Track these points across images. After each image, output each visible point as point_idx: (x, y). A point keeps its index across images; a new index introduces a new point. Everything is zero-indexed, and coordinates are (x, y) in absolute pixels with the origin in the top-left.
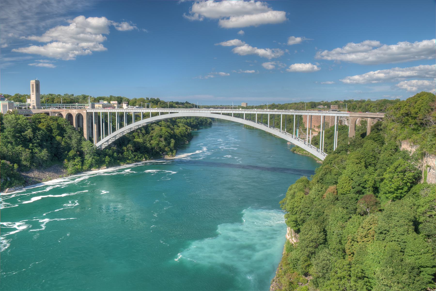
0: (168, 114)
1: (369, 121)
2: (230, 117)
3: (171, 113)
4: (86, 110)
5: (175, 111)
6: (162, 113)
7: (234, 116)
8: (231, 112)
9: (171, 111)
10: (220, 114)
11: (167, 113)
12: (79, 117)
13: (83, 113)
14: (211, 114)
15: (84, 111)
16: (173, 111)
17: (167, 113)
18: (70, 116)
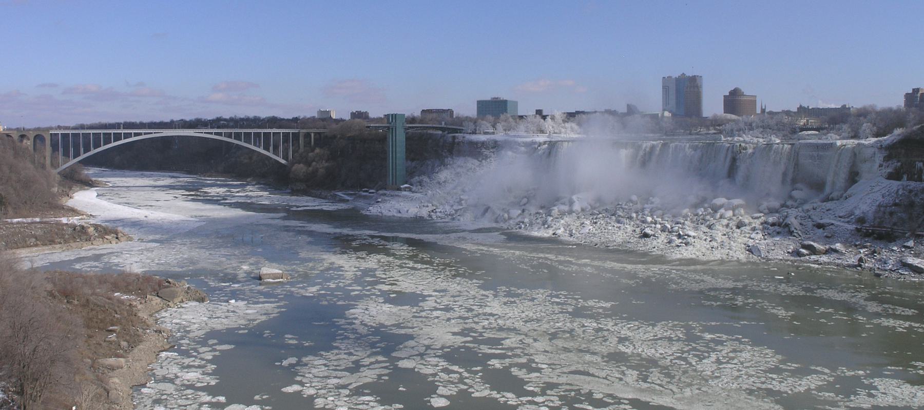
2: (211, 135)
3: (155, 133)
6: (145, 134)
7: (214, 134)
10: (202, 133)
11: (152, 133)
17: (152, 133)
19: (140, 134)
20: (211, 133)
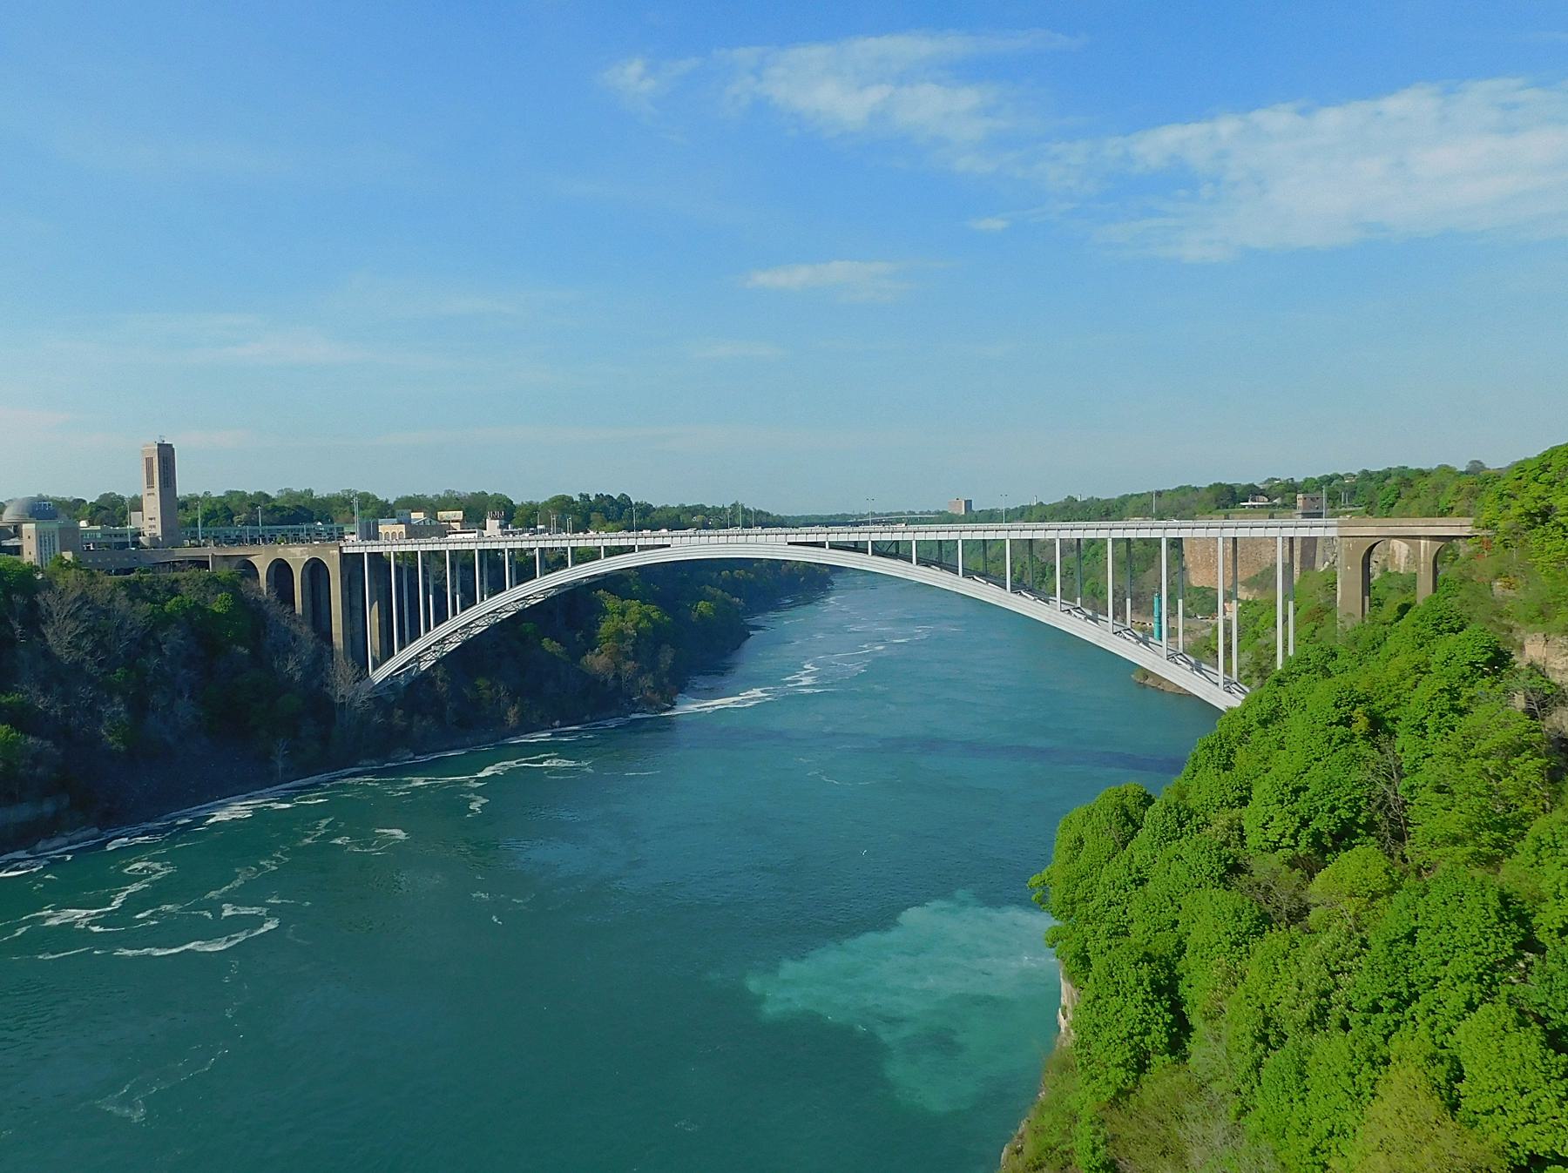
0: (634, 551)
1: (1425, 552)
3: (642, 548)
4: (341, 547)
5: (659, 542)
6: (612, 552)
8: (864, 537)
9: (641, 542)
10: (821, 545)
11: (631, 549)
12: (316, 569)
14: (790, 547)
15: (331, 552)
17: (631, 549)
18: (281, 569)
19: (591, 555)
20: (857, 547)
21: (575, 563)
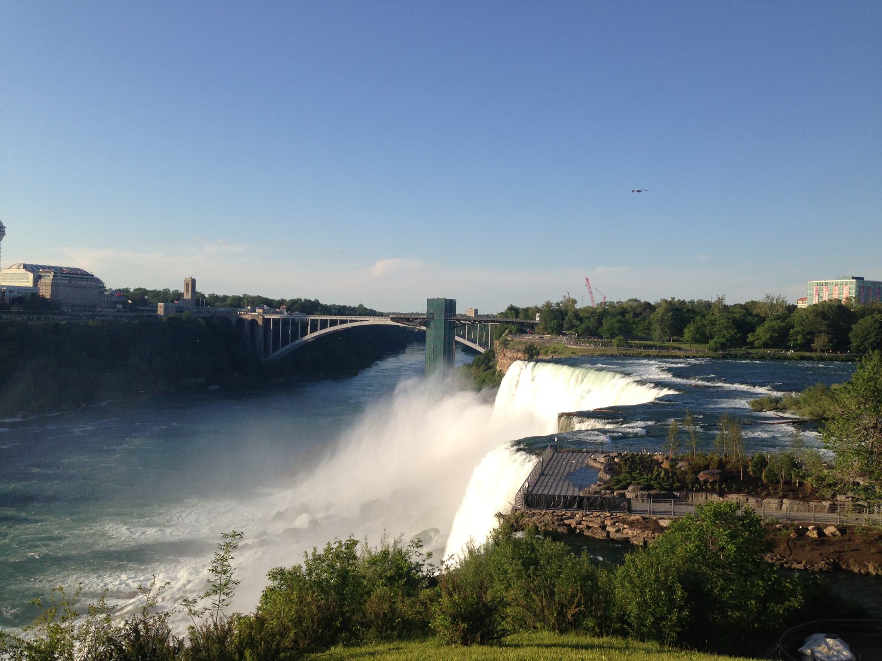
3: (360, 321)
6: (352, 321)
9: (360, 319)
11: (357, 321)
13: (258, 318)
16: (363, 319)
17: (357, 321)
21: (340, 324)
